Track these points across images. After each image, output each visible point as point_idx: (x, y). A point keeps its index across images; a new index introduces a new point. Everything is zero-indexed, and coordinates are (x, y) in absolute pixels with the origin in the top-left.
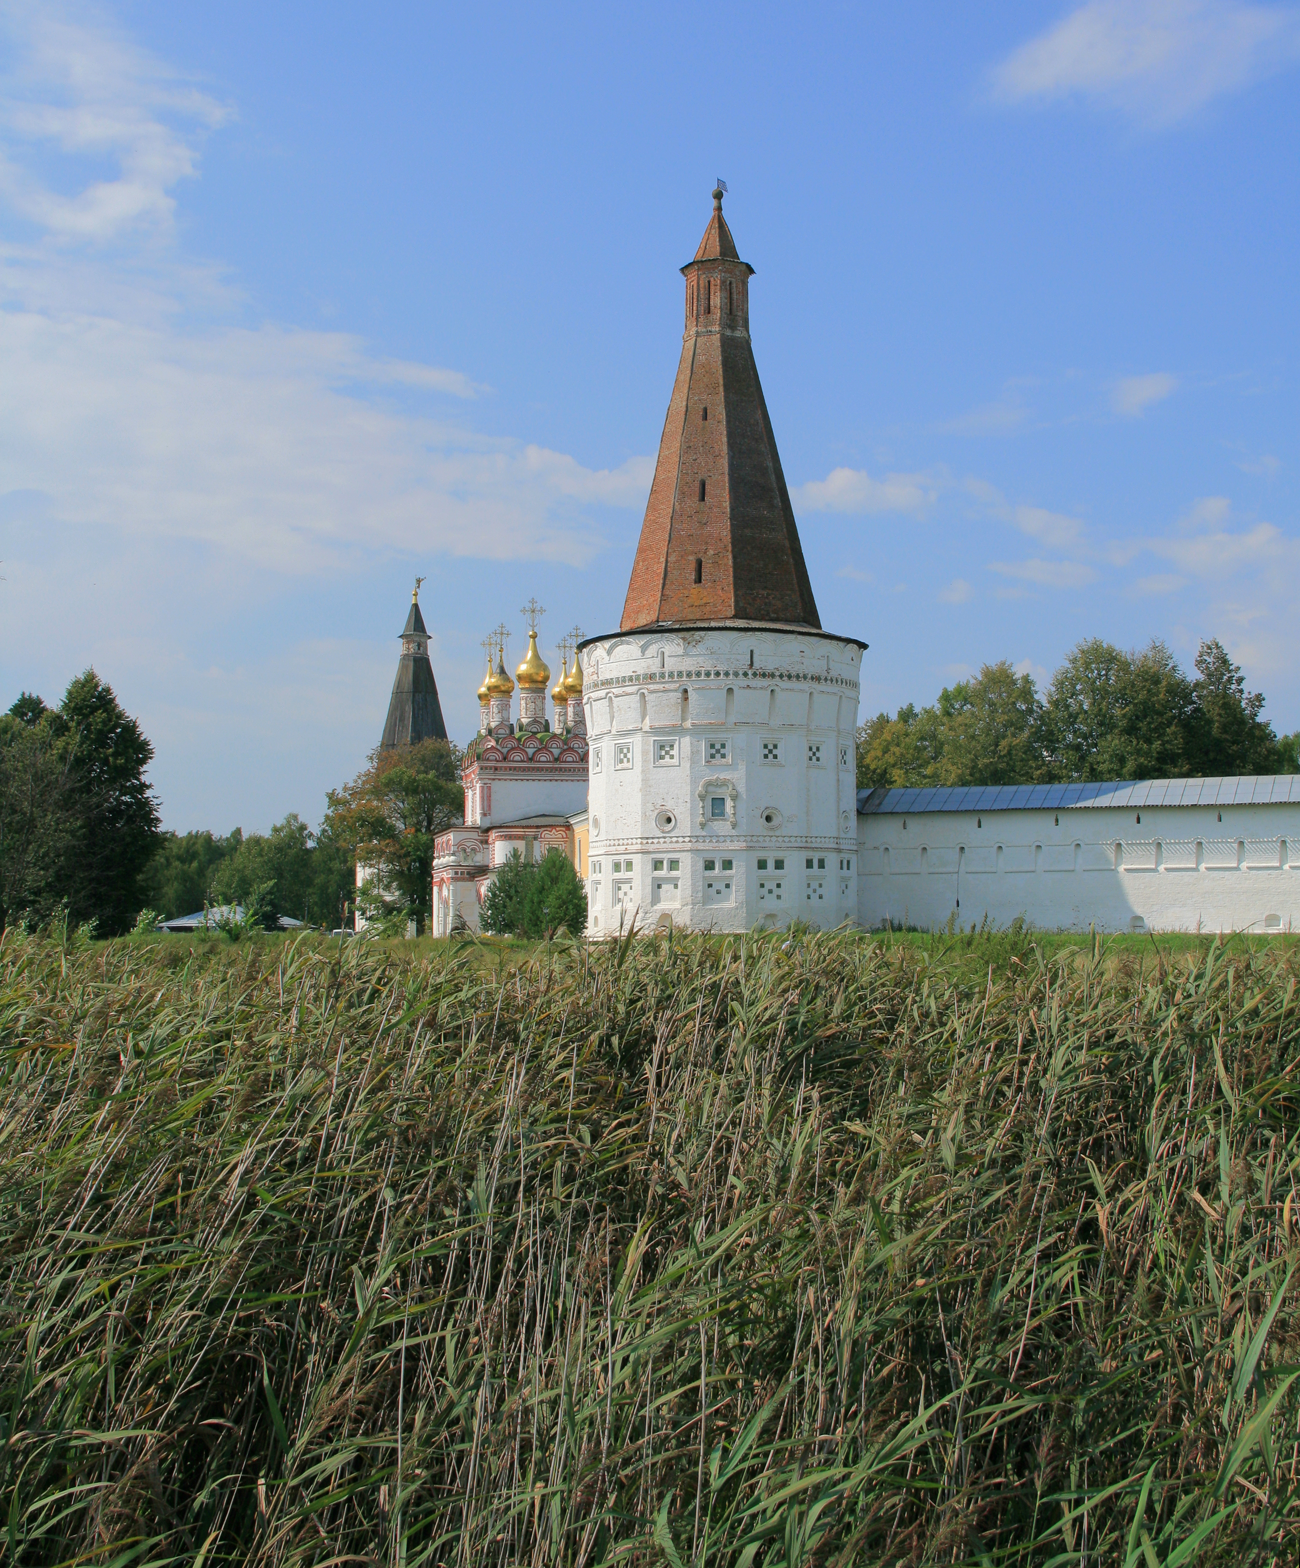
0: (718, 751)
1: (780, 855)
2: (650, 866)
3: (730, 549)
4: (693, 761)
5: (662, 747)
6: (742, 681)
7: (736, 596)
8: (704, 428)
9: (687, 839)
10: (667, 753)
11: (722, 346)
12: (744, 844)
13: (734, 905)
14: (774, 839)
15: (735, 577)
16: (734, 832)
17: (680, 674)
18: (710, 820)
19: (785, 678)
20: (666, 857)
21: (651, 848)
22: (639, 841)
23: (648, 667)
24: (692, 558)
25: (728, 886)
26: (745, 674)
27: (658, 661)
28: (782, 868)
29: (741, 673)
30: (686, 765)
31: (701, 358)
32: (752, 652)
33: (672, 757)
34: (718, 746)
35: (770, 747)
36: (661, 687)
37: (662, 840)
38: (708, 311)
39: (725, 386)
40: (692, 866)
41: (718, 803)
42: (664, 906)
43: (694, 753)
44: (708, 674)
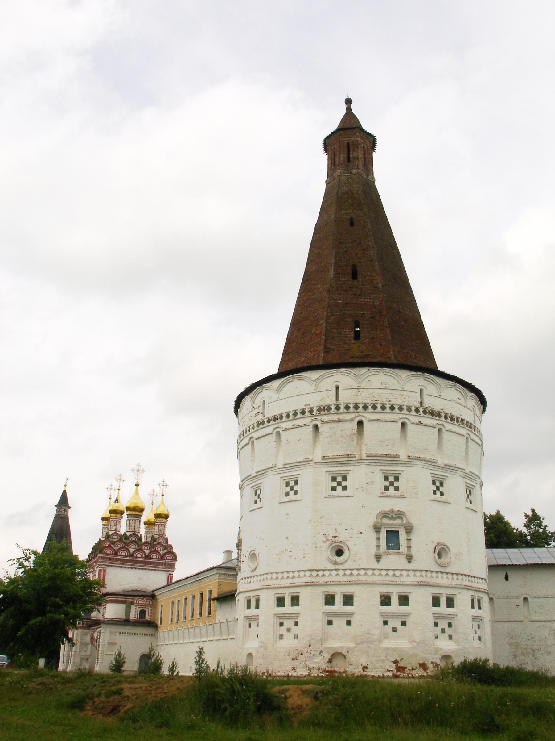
0: (391, 484)
25: (404, 624)
36: (335, 417)
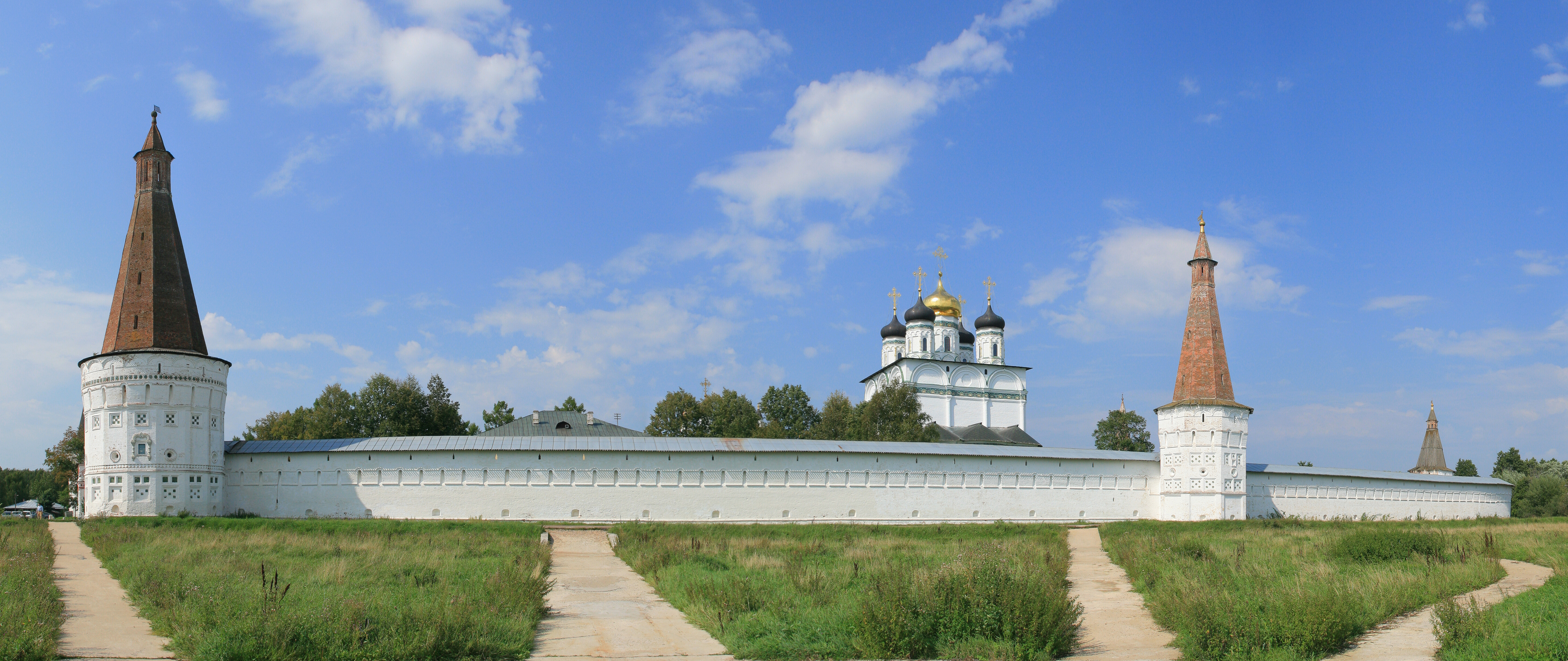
0: (142, 419)
1: (175, 474)
2: (108, 480)
3: (152, 309)
4: (129, 425)
5: (114, 417)
6: (154, 381)
7: (154, 335)
8: (142, 244)
9: (126, 466)
10: (116, 420)
11: (153, 198)
12: (155, 469)
13: (150, 501)
14: (172, 466)
15: (154, 325)
16: (150, 462)
17: (122, 377)
18: (138, 456)
19: (178, 379)
20: (115, 475)
21: (108, 470)
22: (103, 467)
23: (106, 375)
24: (133, 315)
25: (147, 491)
26: (156, 377)
27: (110, 371)
28: (176, 481)
29: (153, 376)
30: (125, 426)
31: (142, 206)
32: (160, 365)
33: (119, 422)
34: (142, 416)
35: (170, 416)
36: (112, 385)
37: (114, 467)
38: (146, 179)
39: (154, 220)
40: (128, 480)
41: (142, 447)
42: (114, 501)
43: (129, 420)
44: (136, 377)
